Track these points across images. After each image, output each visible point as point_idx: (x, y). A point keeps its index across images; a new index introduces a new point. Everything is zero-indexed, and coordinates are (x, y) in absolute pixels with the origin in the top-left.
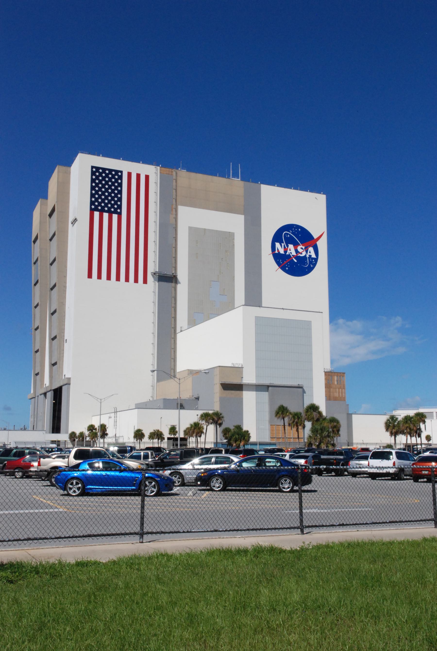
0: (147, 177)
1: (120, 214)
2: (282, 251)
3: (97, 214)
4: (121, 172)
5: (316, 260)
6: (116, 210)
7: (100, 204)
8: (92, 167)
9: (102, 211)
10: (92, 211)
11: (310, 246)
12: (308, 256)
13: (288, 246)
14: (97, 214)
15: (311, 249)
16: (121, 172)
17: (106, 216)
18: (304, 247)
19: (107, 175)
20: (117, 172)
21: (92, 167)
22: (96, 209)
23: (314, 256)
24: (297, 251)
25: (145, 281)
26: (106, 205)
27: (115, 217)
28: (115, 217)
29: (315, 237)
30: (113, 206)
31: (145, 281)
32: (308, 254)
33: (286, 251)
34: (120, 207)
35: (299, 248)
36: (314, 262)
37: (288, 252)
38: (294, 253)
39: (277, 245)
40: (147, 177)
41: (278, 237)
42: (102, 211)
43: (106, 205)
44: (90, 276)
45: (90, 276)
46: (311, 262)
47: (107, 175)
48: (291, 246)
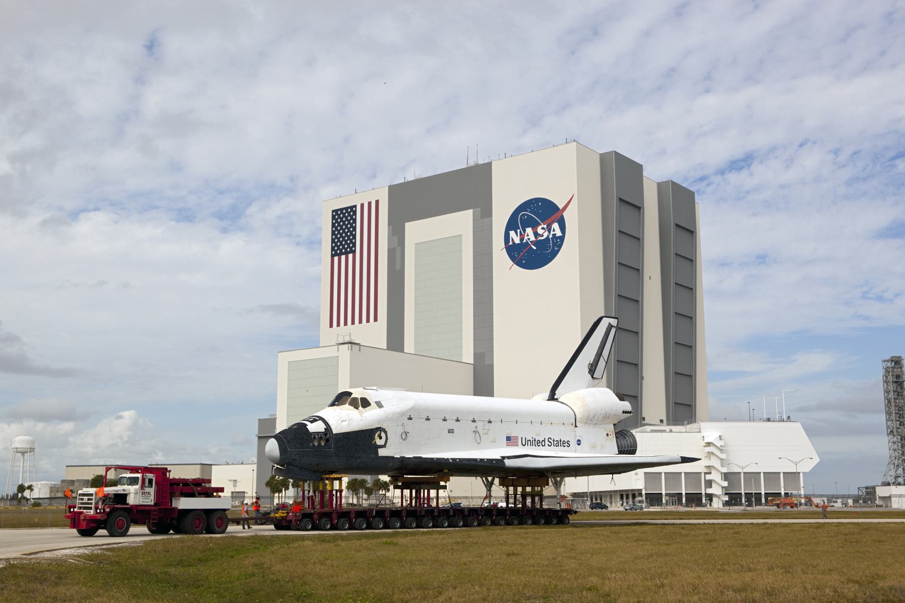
0: (377, 202)
1: (354, 252)
2: (517, 240)
3: (336, 258)
4: (355, 206)
5: (562, 238)
6: (351, 248)
7: (339, 249)
8: (333, 211)
9: (341, 254)
10: (333, 256)
11: (553, 222)
12: (551, 236)
13: (525, 231)
14: (336, 258)
15: (556, 226)
16: (355, 206)
17: (343, 257)
18: (545, 226)
19: (344, 214)
20: (351, 207)
21: (333, 211)
22: (336, 255)
23: (559, 234)
24: (536, 234)
25: (376, 320)
26: (344, 247)
27: (350, 256)
28: (350, 256)
29: (561, 208)
30: (349, 246)
31: (376, 320)
32: (552, 233)
33: (522, 240)
34: (354, 245)
35: (540, 231)
36: (558, 242)
37: (526, 238)
38: (533, 238)
39: (512, 233)
40: (377, 202)
41: (512, 225)
42: (339, 255)
43: (343, 246)
44: (331, 326)
45: (331, 326)
46: (554, 244)
47: (344, 214)
48: (529, 230)
